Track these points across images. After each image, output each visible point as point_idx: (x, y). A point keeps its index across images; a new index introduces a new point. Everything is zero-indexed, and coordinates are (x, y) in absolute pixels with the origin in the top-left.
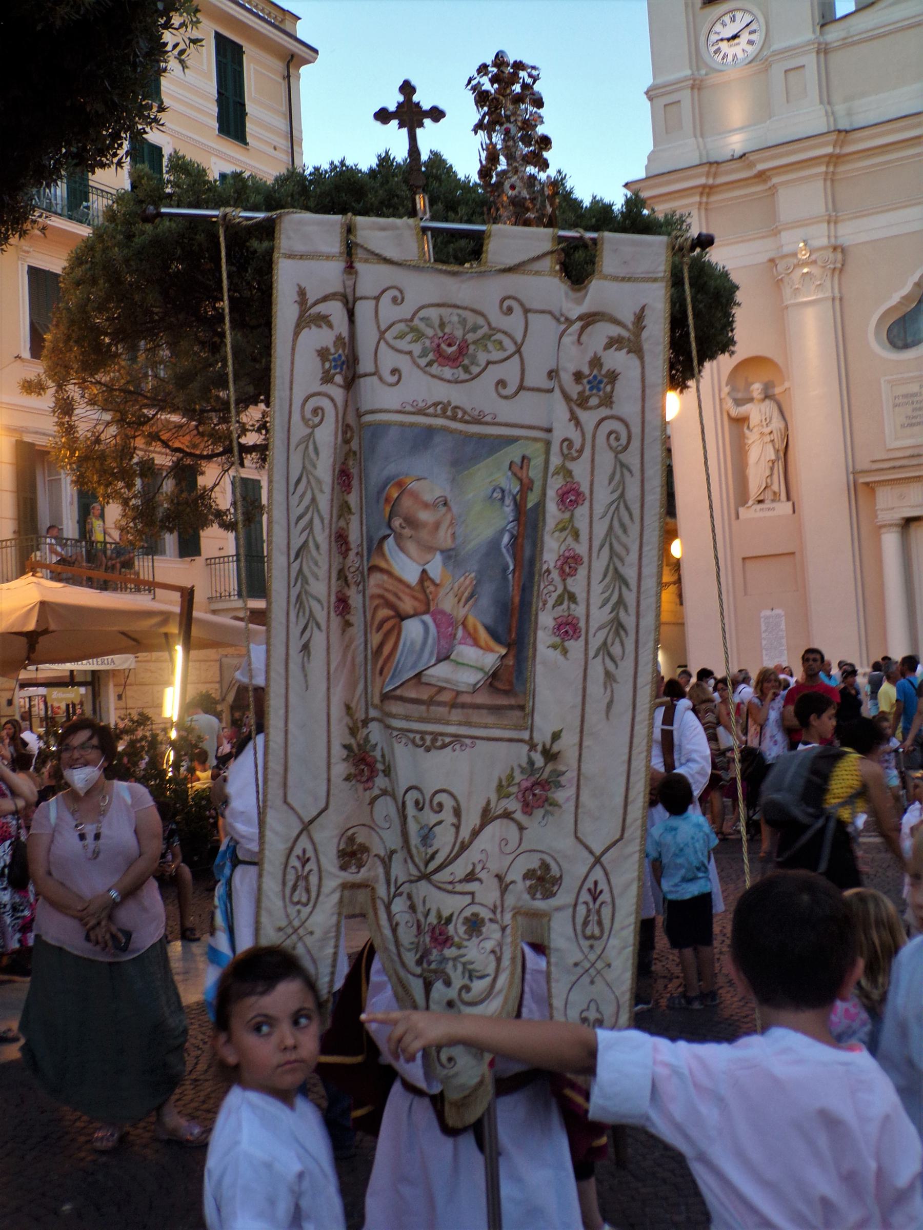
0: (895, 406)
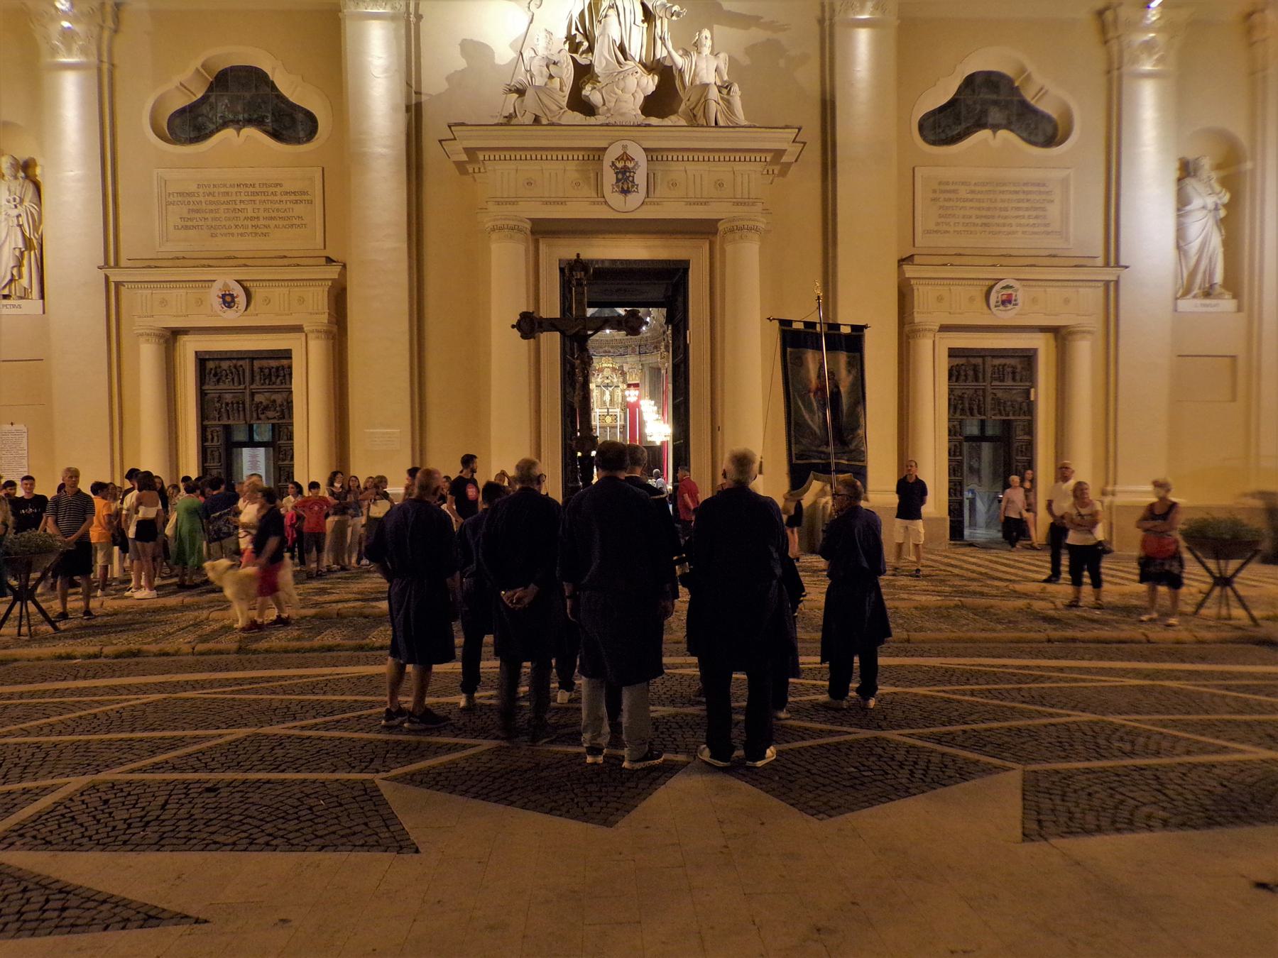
0: (168, 204)
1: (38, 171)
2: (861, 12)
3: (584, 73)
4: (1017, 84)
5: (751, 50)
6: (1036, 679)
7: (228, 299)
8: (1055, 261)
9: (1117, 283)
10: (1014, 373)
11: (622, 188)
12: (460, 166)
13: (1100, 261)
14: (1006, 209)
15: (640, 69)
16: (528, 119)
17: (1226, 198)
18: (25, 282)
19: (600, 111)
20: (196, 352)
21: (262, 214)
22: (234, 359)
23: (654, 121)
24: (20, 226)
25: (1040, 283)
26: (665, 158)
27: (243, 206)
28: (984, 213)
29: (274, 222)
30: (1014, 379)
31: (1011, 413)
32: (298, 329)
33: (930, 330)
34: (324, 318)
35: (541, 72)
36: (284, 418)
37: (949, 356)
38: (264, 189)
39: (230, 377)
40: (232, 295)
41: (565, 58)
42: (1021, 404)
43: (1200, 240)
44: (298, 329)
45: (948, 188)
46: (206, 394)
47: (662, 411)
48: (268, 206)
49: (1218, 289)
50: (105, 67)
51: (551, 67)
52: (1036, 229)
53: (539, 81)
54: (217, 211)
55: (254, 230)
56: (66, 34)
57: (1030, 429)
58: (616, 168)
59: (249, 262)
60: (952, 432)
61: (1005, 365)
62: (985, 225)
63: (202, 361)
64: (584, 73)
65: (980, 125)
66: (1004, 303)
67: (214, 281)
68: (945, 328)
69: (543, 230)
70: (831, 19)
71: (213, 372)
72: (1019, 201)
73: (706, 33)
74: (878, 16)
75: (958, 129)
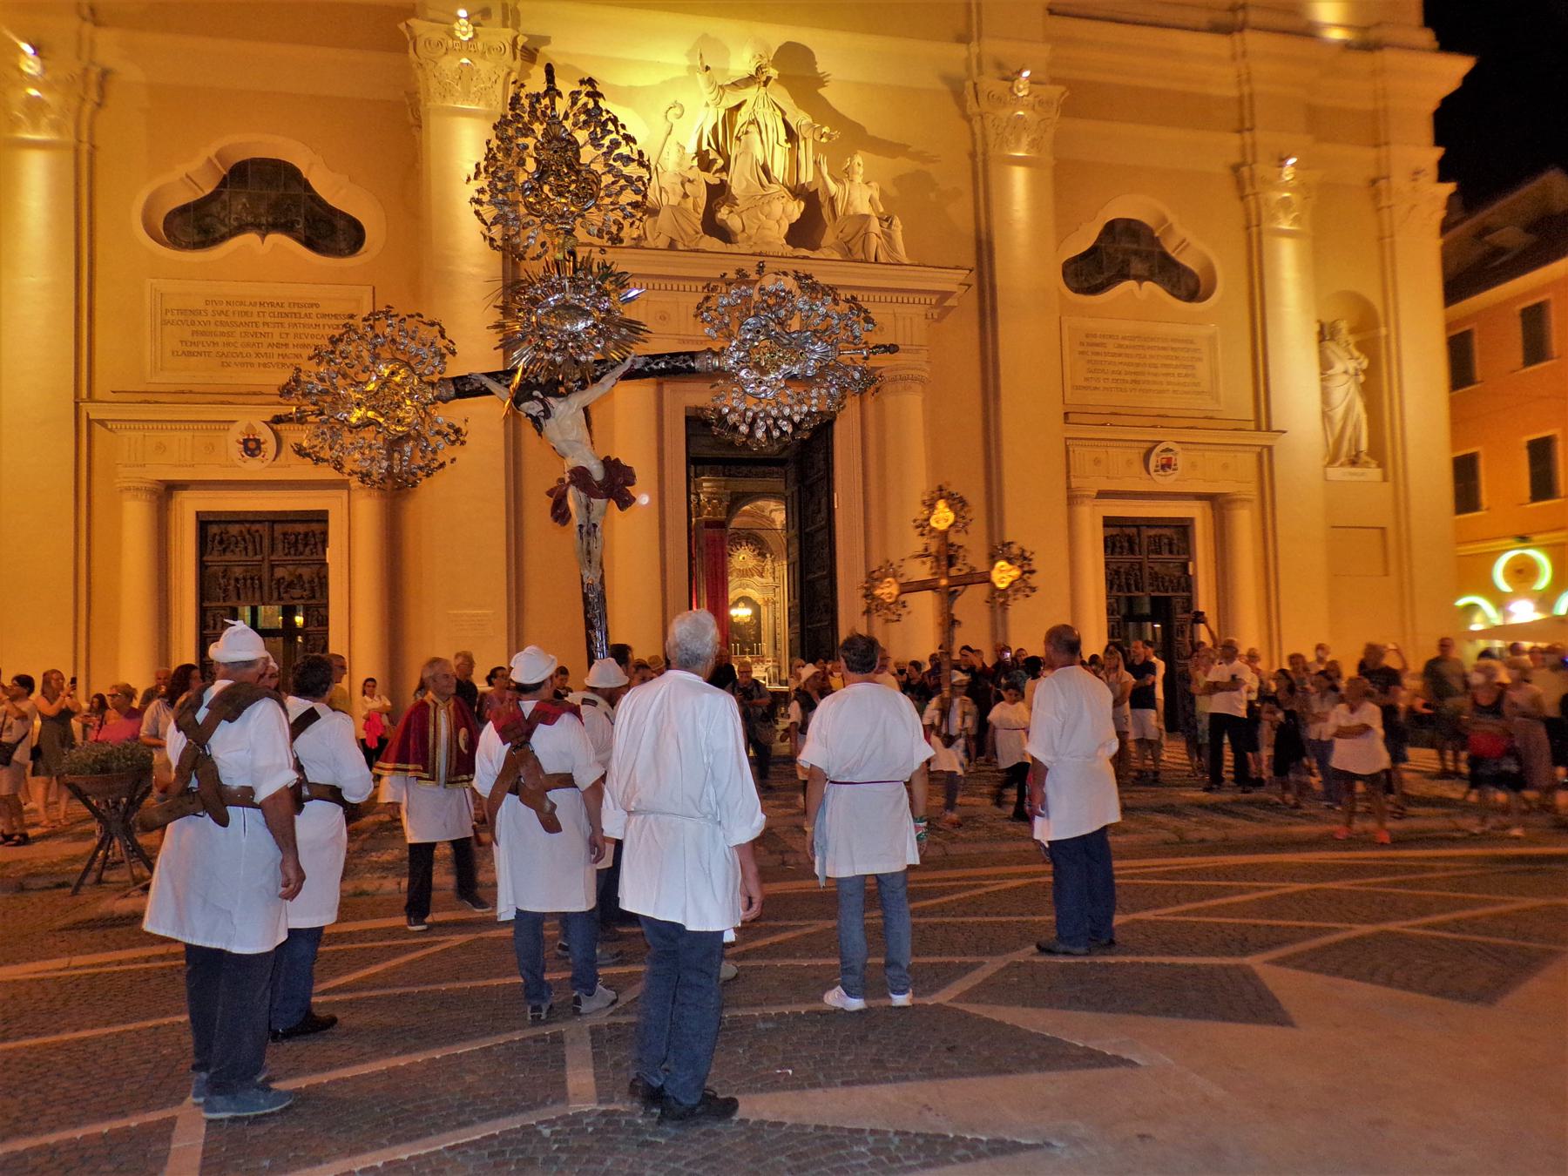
0: (165, 323)
2: (1017, 149)
3: (719, 193)
4: (1157, 234)
5: (898, 181)
6: (1423, 869)
7: (252, 445)
8: (1165, 422)
9: (1270, 448)
10: (1170, 544)
13: (1252, 425)
14: (1156, 366)
16: (662, 242)
17: (1365, 364)
19: (739, 238)
20: (197, 513)
21: (291, 340)
22: (247, 521)
23: (804, 252)
25: (1198, 447)
27: (267, 330)
28: (1132, 369)
30: (1171, 552)
33: (1088, 496)
35: (674, 190)
36: (314, 597)
37: (1105, 526)
38: (296, 310)
39: (242, 545)
40: (258, 442)
43: (1345, 404)
45: (1098, 340)
46: (207, 567)
48: (300, 330)
49: (1364, 457)
50: (85, 147)
51: (687, 185)
52: (1186, 389)
53: (674, 200)
54: (230, 334)
56: (34, 106)
60: (1111, 611)
62: (1135, 381)
63: (205, 523)
64: (719, 193)
65: (1123, 276)
66: (1164, 467)
68: (1102, 495)
70: (984, 154)
71: (218, 538)
72: (1167, 357)
73: (858, 159)
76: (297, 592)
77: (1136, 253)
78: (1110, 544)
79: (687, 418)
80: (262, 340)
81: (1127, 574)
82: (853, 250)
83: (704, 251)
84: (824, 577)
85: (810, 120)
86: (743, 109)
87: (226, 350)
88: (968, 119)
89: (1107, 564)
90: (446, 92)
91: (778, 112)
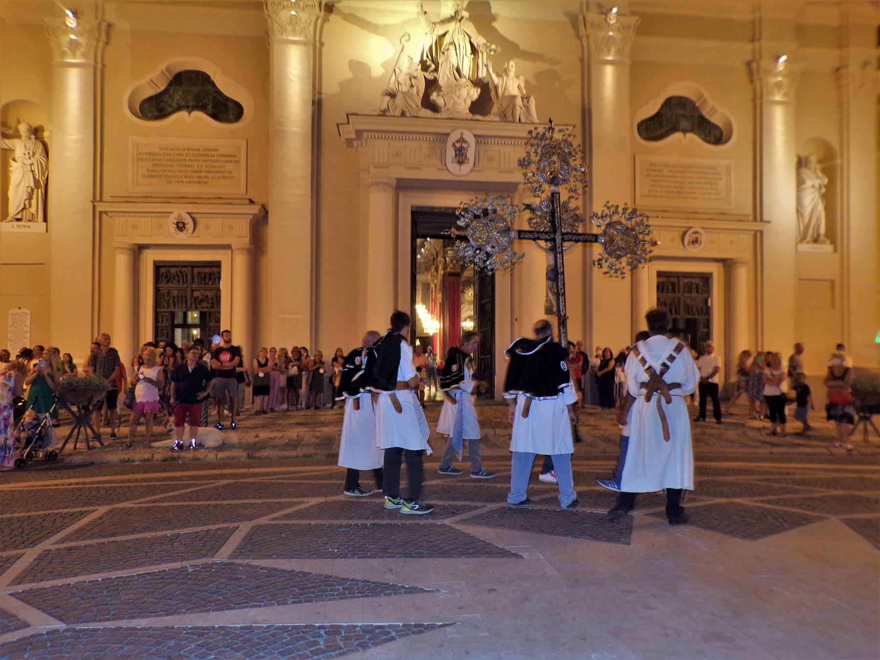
0: (139, 160)
1: (46, 134)
2: (608, 54)
3: (432, 85)
5: (537, 75)
7: (181, 225)
9: (762, 232)
10: (697, 289)
11: (459, 160)
12: (349, 142)
13: (751, 218)
14: (692, 183)
15: (469, 83)
16: (398, 112)
17: (826, 181)
18: (33, 210)
19: (443, 110)
22: (180, 266)
23: (479, 117)
24: (32, 171)
26: (486, 142)
27: (190, 163)
28: (678, 185)
29: (213, 175)
30: (697, 292)
31: (696, 314)
32: (227, 247)
34: (247, 241)
35: (405, 83)
37: (658, 276)
38: (207, 152)
40: (184, 223)
41: (420, 74)
42: (702, 308)
44: (227, 247)
46: (159, 290)
47: (432, 311)
48: (209, 163)
49: (822, 238)
50: (99, 66)
51: (413, 80)
53: (405, 88)
54: (172, 166)
55: (198, 180)
56: (73, 45)
57: (708, 324)
58: (455, 146)
59: (196, 201)
61: (691, 283)
62: (679, 193)
63: (158, 267)
64: (432, 85)
65: (674, 129)
66: (693, 242)
67: (171, 213)
69: (403, 186)
70: (589, 59)
72: (701, 178)
73: (512, 63)
74: (618, 58)
75: (660, 132)
76: (204, 305)
77: (684, 116)
78: (661, 287)
79: (412, 213)
80: (188, 169)
81: (671, 304)
82: (507, 116)
83: (420, 117)
84: (487, 303)
85: (485, 41)
86: (447, 36)
87: (170, 174)
88: (580, 38)
89: (658, 299)
90: (283, 30)
91: (467, 37)
